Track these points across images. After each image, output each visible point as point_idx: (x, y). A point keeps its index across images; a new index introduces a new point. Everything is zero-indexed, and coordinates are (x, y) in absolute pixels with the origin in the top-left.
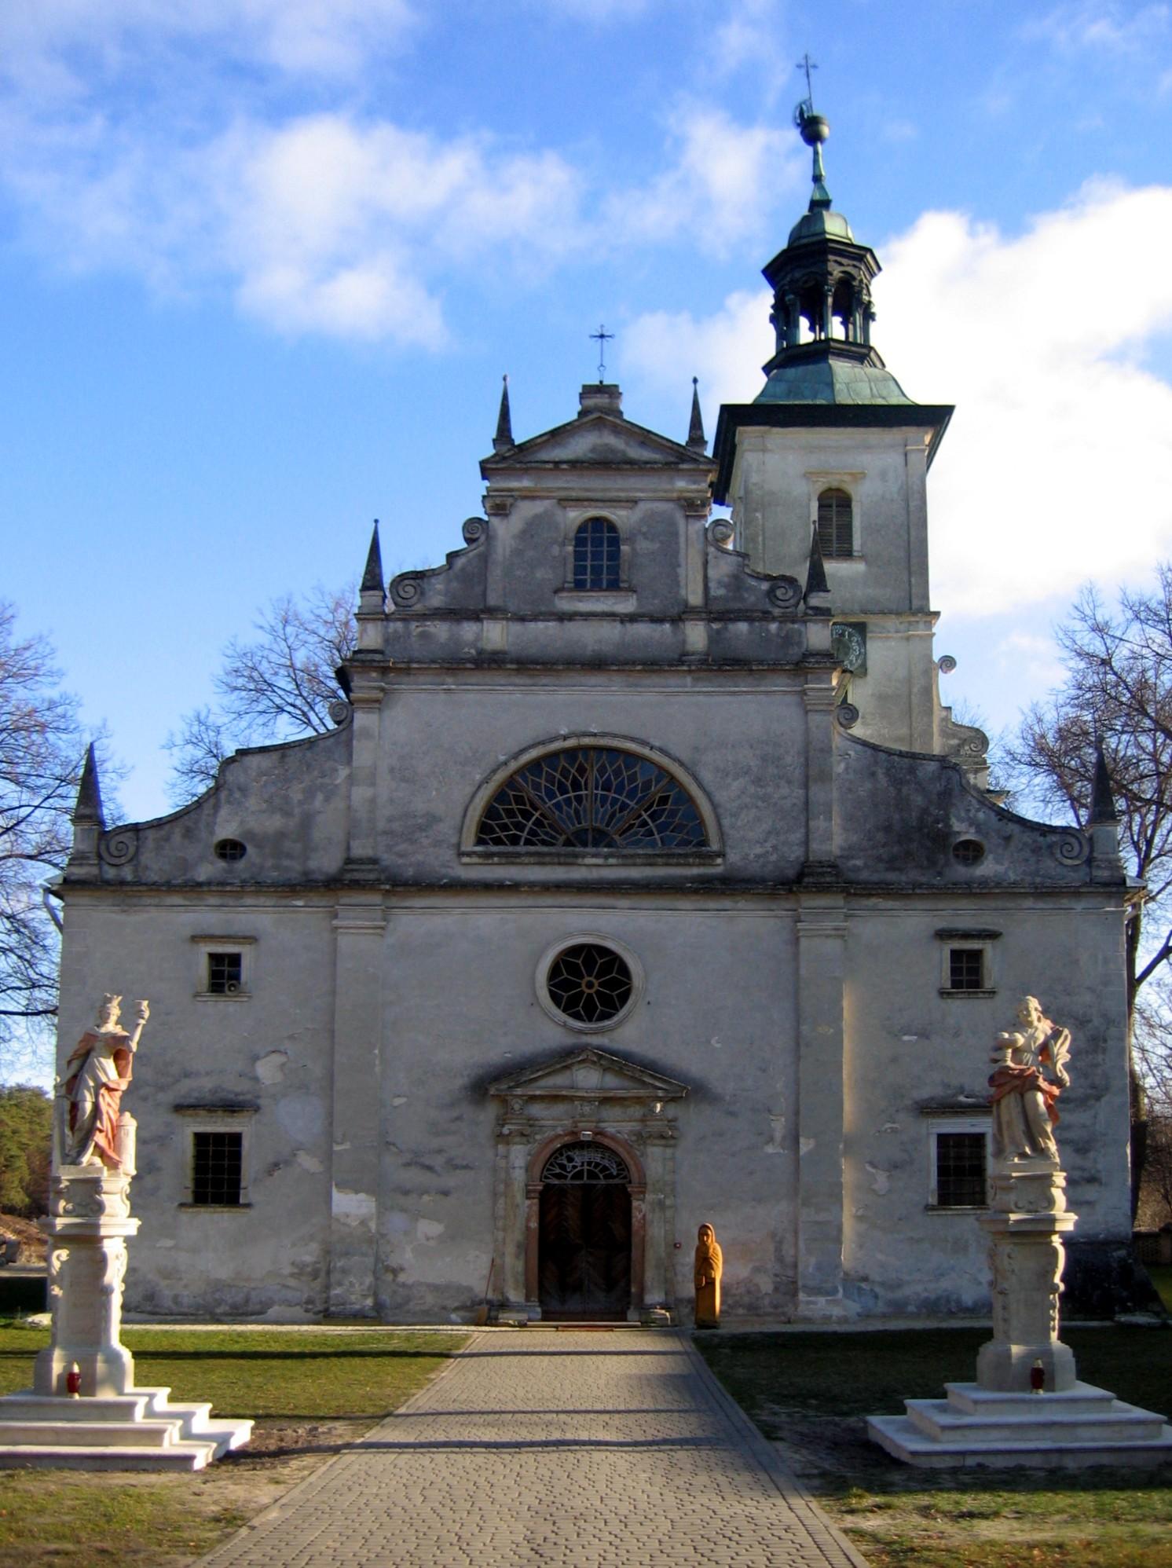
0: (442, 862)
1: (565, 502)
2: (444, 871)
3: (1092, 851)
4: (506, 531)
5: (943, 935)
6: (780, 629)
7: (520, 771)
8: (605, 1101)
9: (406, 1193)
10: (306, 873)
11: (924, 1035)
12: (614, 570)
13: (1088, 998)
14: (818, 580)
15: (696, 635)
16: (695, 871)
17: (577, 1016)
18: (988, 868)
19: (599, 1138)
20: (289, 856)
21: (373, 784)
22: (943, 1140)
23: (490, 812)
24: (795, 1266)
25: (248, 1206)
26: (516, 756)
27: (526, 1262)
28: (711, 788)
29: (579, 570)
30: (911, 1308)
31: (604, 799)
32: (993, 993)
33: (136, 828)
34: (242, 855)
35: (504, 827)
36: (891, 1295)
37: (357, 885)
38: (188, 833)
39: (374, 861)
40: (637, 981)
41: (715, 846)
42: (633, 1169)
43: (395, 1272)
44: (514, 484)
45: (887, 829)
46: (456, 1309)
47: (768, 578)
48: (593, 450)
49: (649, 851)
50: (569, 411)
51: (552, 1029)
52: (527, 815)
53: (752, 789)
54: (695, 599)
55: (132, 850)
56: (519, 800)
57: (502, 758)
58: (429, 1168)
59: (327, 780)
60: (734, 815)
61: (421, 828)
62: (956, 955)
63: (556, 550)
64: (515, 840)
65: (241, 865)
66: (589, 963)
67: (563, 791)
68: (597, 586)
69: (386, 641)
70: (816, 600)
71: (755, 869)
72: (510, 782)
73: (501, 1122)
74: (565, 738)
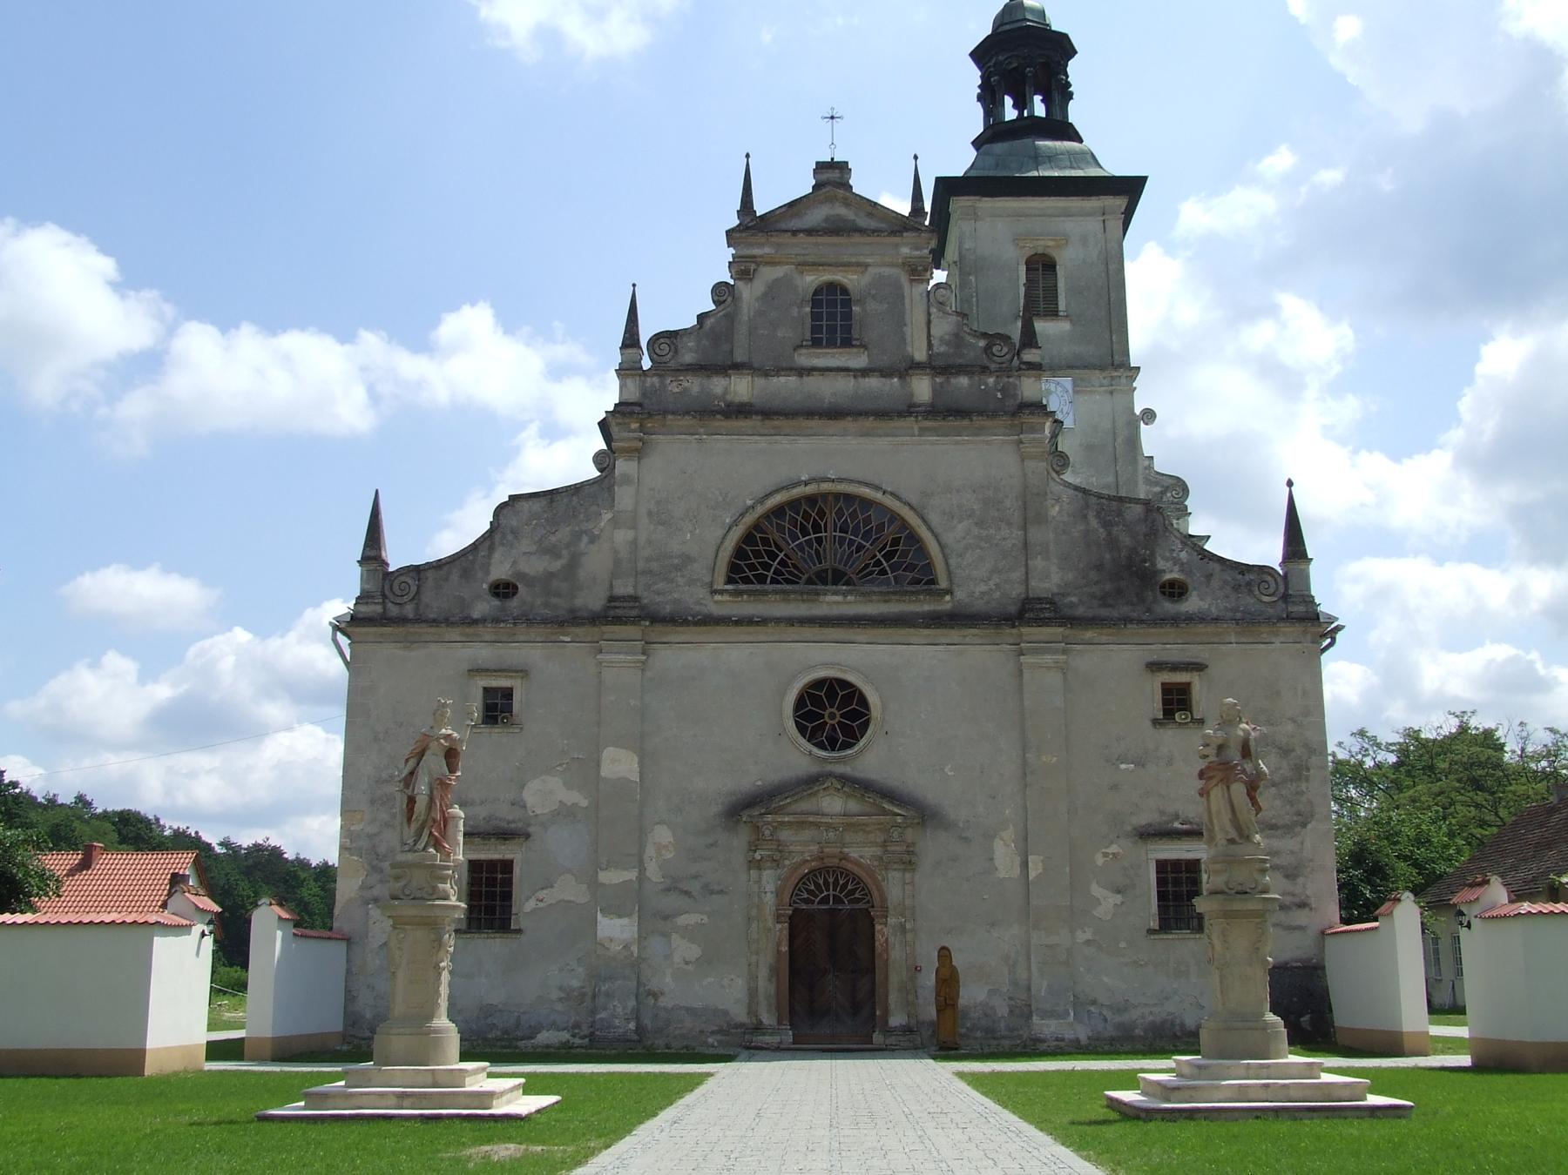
0: (698, 598)
1: (804, 265)
2: (698, 608)
3: (1287, 588)
4: (749, 294)
5: (1155, 667)
6: (997, 382)
7: (766, 516)
8: (849, 827)
9: (666, 918)
10: (572, 611)
11: (1140, 763)
12: (848, 329)
13: (1290, 727)
14: (1029, 338)
15: (922, 388)
16: (926, 608)
17: (821, 746)
18: (1193, 604)
19: (844, 864)
20: (558, 595)
21: (634, 527)
22: (1162, 866)
23: (739, 553)
24: (1029, 989)
25: (519, 931)
26: (762, 500)
27: (778, 988)
28: (939, 530)
29: (815, 329)
30: (1138, 1032)
31: (842, 540)
32: (1201, 721)
33: (416, 570)
34: (514, 594)
35: (752, 567)
36: (1118, 1019)
37: (618, 620)
38: (466, 574)
39: (635, 598)
40: (876, 712)
41: (943, 584)
42: (875, 894)
43: (655, 995)
44: (756, 251)
45: (1099, 567)
46: (713, 1033)
47: (985, 335)
48: (826, 220)
49: (884, 589)
50: (804, 185)
51: (799, 757)
52: (773, 556)
53: (976, 531)
54: (920, 355)
55: (414, 589)
56: (766, 542)
57: (749, 503)
58: (687, 893)
59: (590, 525)
60: (960, 556)
61: (677, 568)
62: (1167, 689)
63: (795, 311)
64: (761, 579)
65: (514, 603)
66: (832, 694)
67: (805, 533)
68: (831, 343)
69: (644, 394)
70: (1030, 356)
71: (979, 606)
72: (757, 526)
73: (753, 847)
74: (806, 484)
